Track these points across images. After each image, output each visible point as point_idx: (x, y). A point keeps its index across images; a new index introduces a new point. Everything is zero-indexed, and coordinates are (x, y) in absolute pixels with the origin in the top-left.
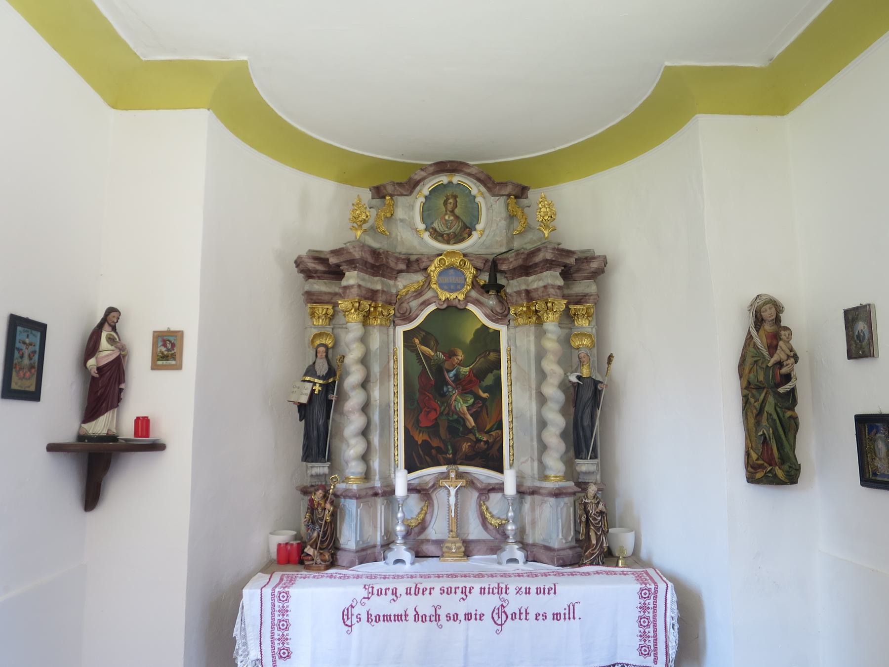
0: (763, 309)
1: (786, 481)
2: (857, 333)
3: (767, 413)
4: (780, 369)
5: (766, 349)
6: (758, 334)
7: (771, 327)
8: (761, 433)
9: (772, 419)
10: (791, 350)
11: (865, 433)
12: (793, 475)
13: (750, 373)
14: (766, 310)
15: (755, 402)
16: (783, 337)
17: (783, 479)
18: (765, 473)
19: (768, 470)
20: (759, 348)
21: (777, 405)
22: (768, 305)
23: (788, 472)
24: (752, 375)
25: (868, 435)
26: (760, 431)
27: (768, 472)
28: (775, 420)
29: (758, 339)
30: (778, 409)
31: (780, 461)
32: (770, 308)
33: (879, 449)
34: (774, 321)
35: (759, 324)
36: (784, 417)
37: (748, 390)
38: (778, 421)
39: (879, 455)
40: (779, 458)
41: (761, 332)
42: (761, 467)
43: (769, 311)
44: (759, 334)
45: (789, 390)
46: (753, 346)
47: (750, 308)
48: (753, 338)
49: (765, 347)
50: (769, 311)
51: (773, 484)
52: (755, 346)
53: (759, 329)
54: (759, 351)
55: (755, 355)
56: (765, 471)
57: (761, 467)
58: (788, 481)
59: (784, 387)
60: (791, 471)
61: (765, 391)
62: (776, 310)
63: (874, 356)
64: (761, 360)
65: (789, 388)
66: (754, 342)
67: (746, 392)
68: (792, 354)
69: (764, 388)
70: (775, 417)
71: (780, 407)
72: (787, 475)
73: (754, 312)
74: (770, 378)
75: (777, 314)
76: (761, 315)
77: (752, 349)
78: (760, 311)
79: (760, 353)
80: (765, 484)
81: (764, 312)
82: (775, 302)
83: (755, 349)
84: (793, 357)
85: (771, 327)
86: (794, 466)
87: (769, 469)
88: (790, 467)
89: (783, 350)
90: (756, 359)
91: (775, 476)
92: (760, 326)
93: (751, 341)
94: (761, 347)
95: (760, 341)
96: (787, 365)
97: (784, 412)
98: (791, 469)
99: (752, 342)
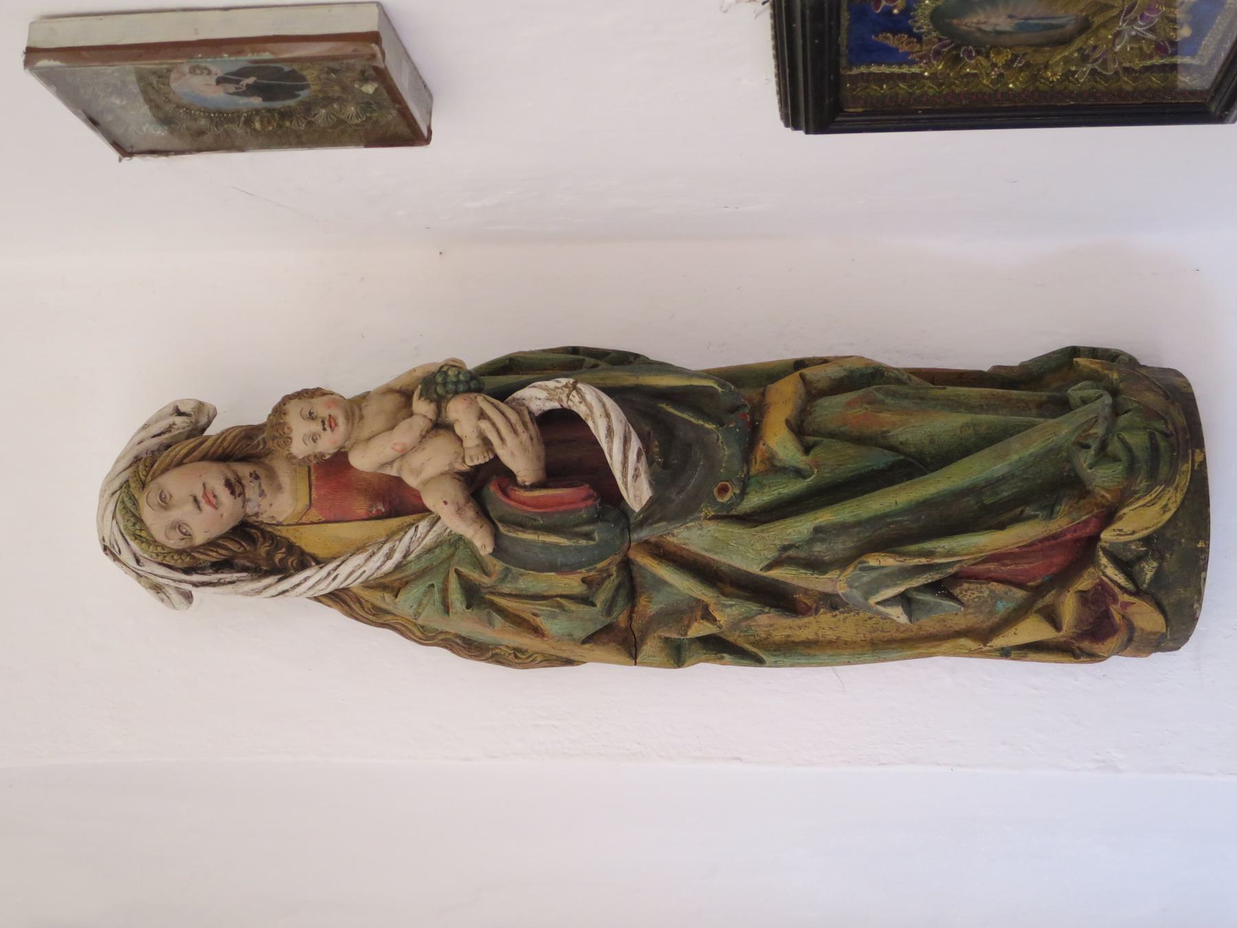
0: (174, 542)
1: (1183, 480)
2: (256, 101)
3: (769, 567)
4: (508, 476)
5: (404, 529)
6: (321, 562)
7: (279, 488)
8: (897, 614)
9: (811, 541)
10: (403, 396)
11: (902, 77)
12: (1152, 437)
13: (537, 631)
14: (178, 526)
15: (707, 616)
16: (327, 444)
17: (1172, 498)
18: (1138, 593)
19: (1121, 579)
20: (399, 567)
21: (730, 506)
22: (149, 515)
23: (1131, 469)
24: (553, 626)
25: (911, 63)
26: (885, 617)
27: (1130, 576)
28: (817, 530)
29: (345, 570)
30: (754, 500)
31: (1062, 508)
32: (165, 503)
33: (1021, 28)
34: (244, 470)
35: (263, 550)
36: (799, 473)
37: (643, 639)
38: (825, 517)
39: (1062, 26)
40: (1051, 515)
41: (311, 539)
42: (1097, 600)
43: (184, 512)
44: (320, 553)
45: (635, 444)
46: (388, 597)
47: (175, 597)
48: (345, 590)
49: (389, 537)
50: (184, 512)
51: (1205, 551)
52: (391, 585)
53: (291, 548)
54: (414, 568)
55: (437, 596)
56: (1126, 598)
57: (1097, 600)
58: (1186, 467)
59: (618, 474)
60: (1128, 449)
61: (645, 561)
62: (180, 463)
63: (374, 37)
64: (465, 570)
65: (626, 441)
66: (369, 585)
67: (650, 647)
68: (422, 407)
69: (627, 565)
70: (798, 528)
71: (743, 493)
72: (1153, 475)
73: (196, 578)
74: (564, 541)
75: (203, 458)
76: (212, 544)
77: (404, 604)
78: (180, 552)
79: (424, 563)
80: (1199, 593)
81: (187, 535)
82: (137, 459)
83: (406, 583)
84: (440, 402)
85: (279, 488)
86: (1099, 430)
87: (1111, 571)
88: (1103, 455)
89: (403, 454)
90: (456, 597)
91: (1154, 543)
92: (276, 542)
93: (358, 600)
94: (389, 557)
95: (359, 559)
96: (486, 443)
97: (776, 469)
98: (1115, 447)
99: (366, 595)
